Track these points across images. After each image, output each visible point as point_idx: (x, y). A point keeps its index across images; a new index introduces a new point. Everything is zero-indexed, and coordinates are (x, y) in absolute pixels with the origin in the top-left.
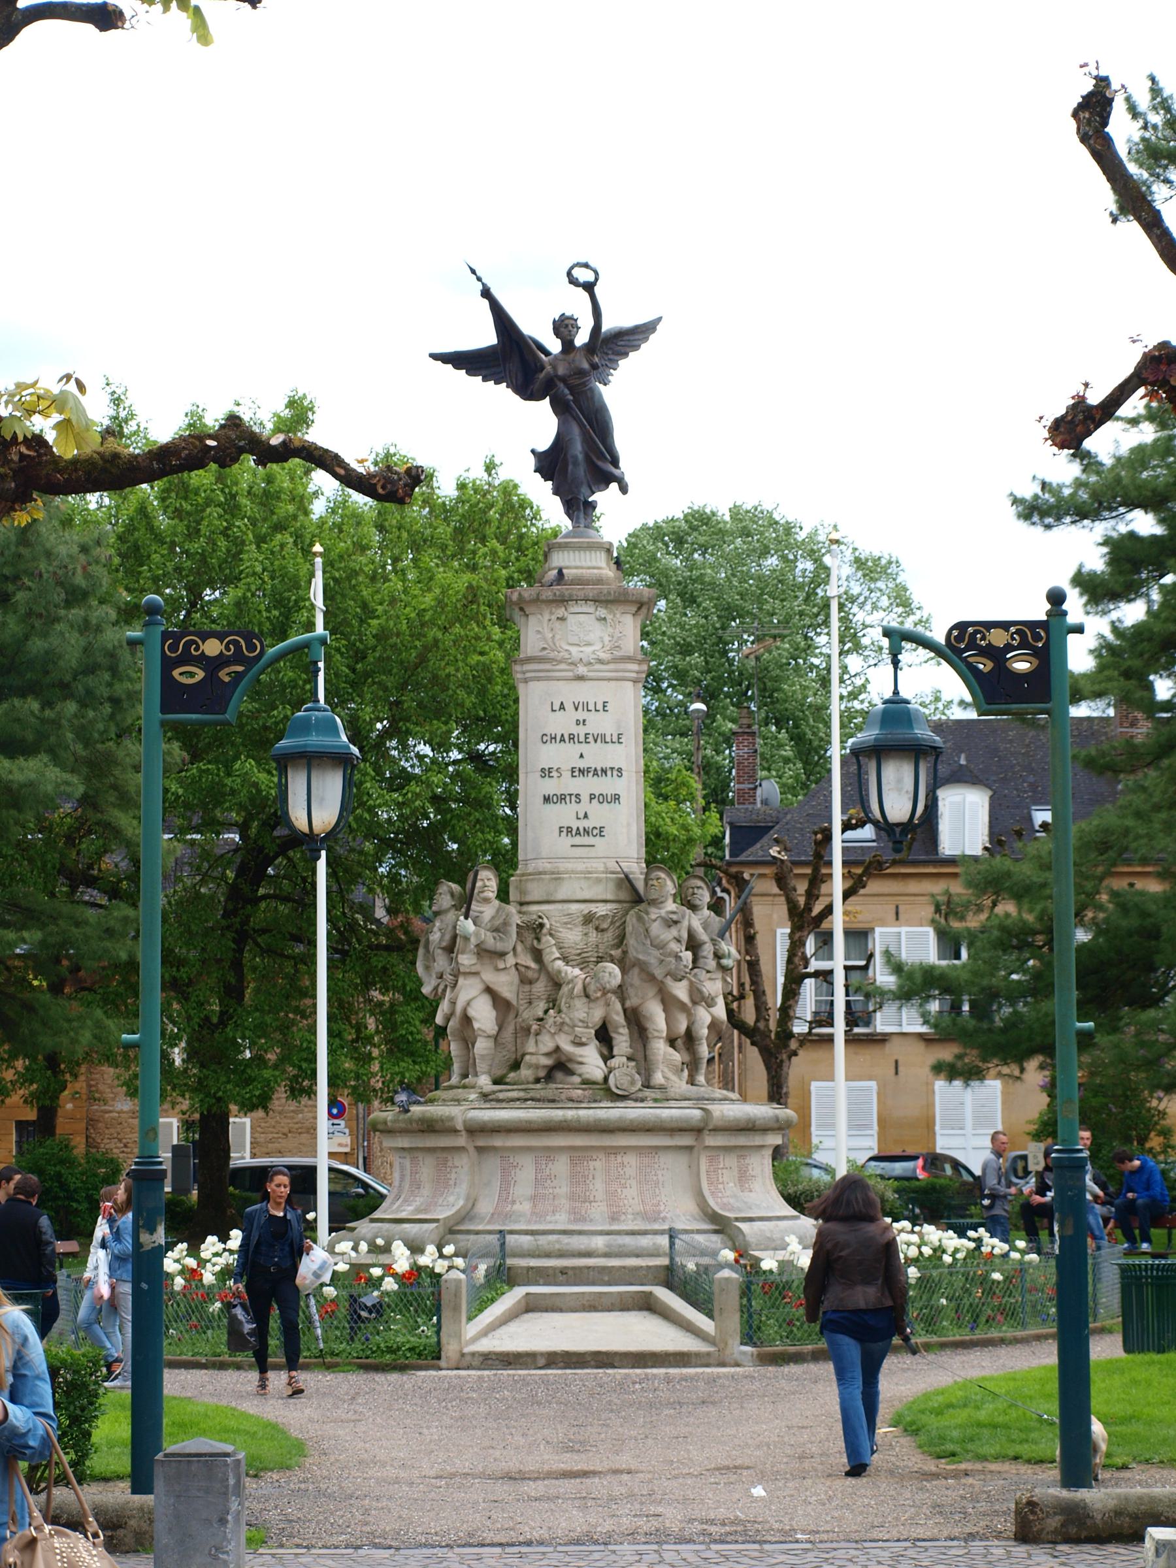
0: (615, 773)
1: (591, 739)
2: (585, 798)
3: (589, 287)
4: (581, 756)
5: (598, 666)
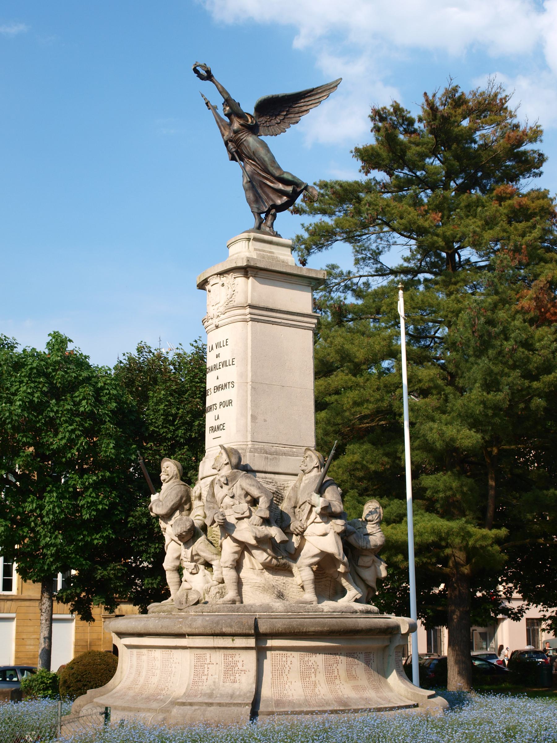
0: (231, 385)
1: (221, 366)
2: (218, 406)
3: (209, 77)
4: (218, 378)
5: (222, 316)
